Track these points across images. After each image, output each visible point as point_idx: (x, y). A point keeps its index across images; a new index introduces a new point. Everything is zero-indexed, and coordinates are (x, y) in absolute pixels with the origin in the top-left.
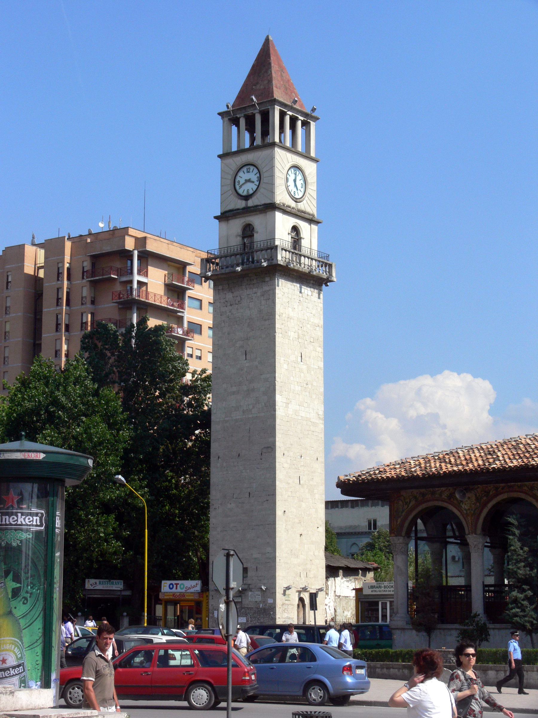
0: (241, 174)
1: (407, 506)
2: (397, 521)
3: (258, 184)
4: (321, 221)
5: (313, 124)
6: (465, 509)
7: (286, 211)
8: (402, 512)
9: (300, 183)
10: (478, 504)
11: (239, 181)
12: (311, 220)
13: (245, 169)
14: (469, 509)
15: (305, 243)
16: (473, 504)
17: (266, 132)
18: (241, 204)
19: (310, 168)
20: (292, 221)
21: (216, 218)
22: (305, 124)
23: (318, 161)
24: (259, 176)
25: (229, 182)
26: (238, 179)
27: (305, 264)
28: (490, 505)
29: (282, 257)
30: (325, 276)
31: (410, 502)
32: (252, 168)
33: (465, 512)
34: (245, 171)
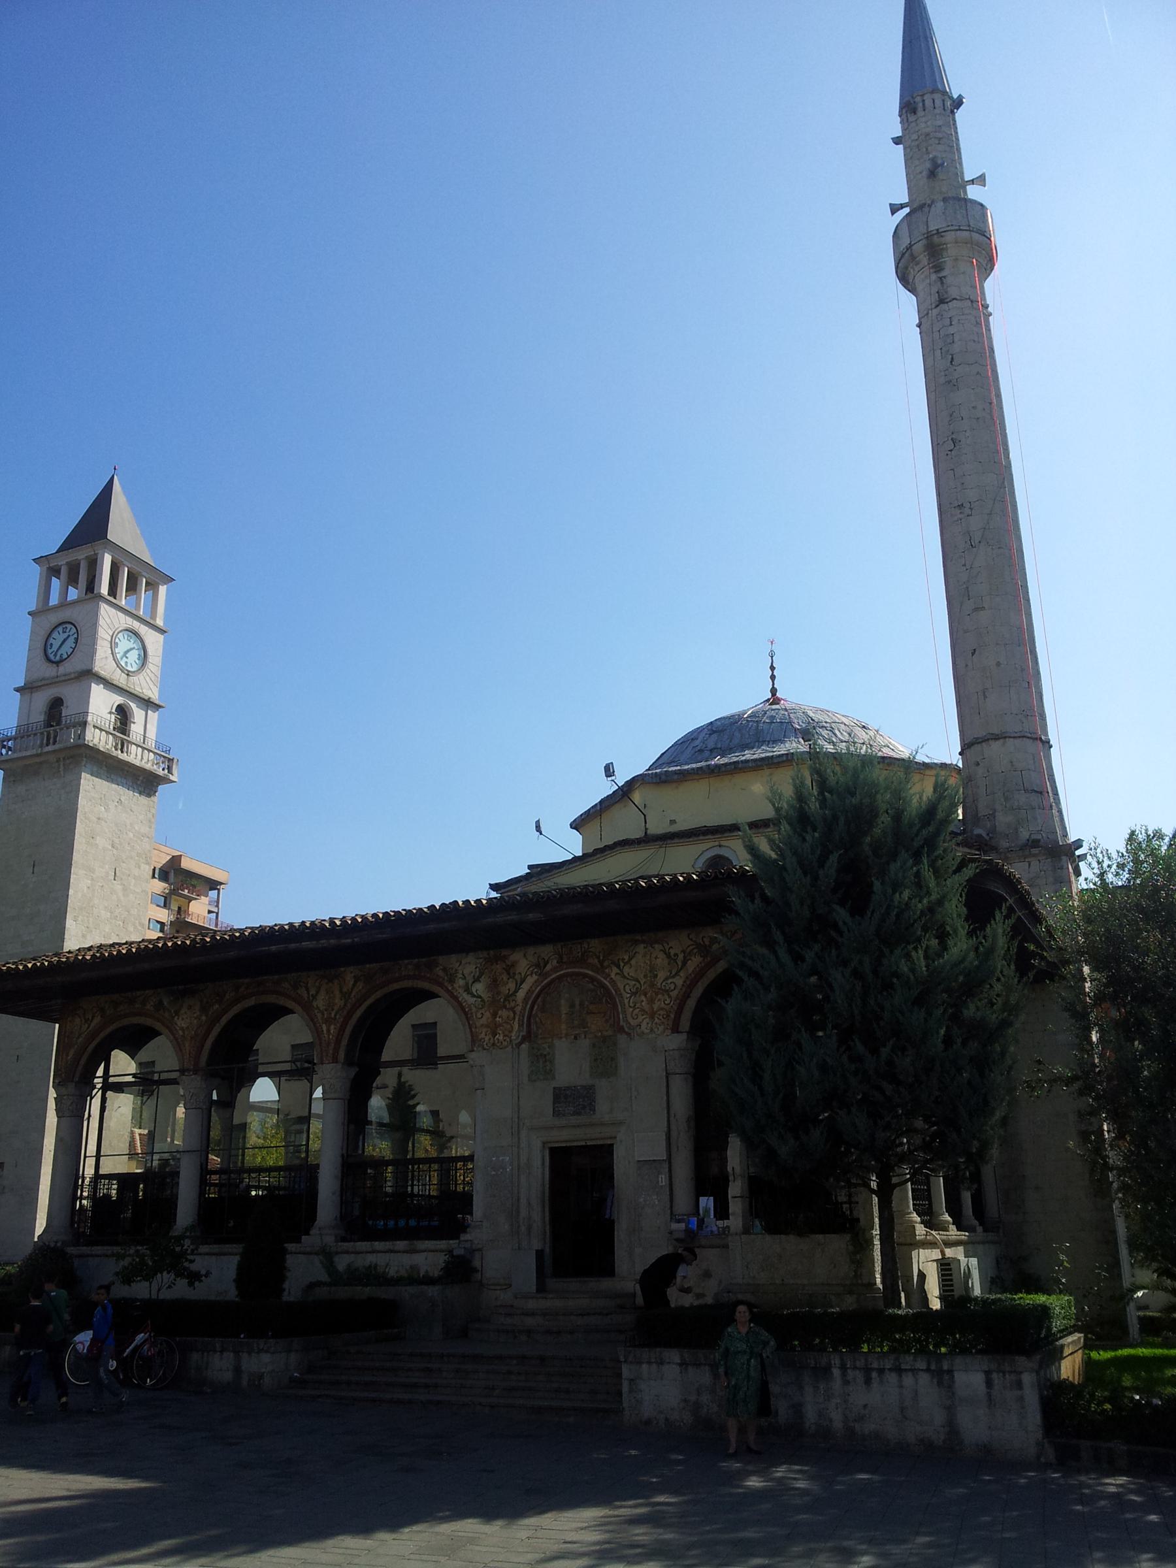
0: (55, 635)
1: (87, 1025)
2: (67, 1055)
3: (73, 647)
4: (161, 704)
5: (163, 590)
6: (182, 1029)
7: (109, 685)
8: (78, 1038)
9: (134, 656)
10: (204, 1018)
11: (52, 644)
12: (148, 704)
13: (60, 629)
14: (188, 1028)
15: (136, 728)
16: (196, 1018)
17: (91, 586)
18: (49, 671)
19: (154, 641)
20: (118, 700)
21: (17, 690)
22: (152, 586)
23: (165, 632)
24: (76, 636)
25: (40, 645)
26: (51, 641)
27: (134, 756)
28: (224, 1020)
29: (96, 738)
30: (160, 772)
31: (93, 1017)
32: (69, 626)
33: (181, 1033)
34: (61, 632)
